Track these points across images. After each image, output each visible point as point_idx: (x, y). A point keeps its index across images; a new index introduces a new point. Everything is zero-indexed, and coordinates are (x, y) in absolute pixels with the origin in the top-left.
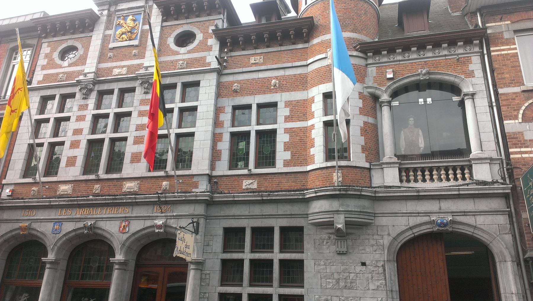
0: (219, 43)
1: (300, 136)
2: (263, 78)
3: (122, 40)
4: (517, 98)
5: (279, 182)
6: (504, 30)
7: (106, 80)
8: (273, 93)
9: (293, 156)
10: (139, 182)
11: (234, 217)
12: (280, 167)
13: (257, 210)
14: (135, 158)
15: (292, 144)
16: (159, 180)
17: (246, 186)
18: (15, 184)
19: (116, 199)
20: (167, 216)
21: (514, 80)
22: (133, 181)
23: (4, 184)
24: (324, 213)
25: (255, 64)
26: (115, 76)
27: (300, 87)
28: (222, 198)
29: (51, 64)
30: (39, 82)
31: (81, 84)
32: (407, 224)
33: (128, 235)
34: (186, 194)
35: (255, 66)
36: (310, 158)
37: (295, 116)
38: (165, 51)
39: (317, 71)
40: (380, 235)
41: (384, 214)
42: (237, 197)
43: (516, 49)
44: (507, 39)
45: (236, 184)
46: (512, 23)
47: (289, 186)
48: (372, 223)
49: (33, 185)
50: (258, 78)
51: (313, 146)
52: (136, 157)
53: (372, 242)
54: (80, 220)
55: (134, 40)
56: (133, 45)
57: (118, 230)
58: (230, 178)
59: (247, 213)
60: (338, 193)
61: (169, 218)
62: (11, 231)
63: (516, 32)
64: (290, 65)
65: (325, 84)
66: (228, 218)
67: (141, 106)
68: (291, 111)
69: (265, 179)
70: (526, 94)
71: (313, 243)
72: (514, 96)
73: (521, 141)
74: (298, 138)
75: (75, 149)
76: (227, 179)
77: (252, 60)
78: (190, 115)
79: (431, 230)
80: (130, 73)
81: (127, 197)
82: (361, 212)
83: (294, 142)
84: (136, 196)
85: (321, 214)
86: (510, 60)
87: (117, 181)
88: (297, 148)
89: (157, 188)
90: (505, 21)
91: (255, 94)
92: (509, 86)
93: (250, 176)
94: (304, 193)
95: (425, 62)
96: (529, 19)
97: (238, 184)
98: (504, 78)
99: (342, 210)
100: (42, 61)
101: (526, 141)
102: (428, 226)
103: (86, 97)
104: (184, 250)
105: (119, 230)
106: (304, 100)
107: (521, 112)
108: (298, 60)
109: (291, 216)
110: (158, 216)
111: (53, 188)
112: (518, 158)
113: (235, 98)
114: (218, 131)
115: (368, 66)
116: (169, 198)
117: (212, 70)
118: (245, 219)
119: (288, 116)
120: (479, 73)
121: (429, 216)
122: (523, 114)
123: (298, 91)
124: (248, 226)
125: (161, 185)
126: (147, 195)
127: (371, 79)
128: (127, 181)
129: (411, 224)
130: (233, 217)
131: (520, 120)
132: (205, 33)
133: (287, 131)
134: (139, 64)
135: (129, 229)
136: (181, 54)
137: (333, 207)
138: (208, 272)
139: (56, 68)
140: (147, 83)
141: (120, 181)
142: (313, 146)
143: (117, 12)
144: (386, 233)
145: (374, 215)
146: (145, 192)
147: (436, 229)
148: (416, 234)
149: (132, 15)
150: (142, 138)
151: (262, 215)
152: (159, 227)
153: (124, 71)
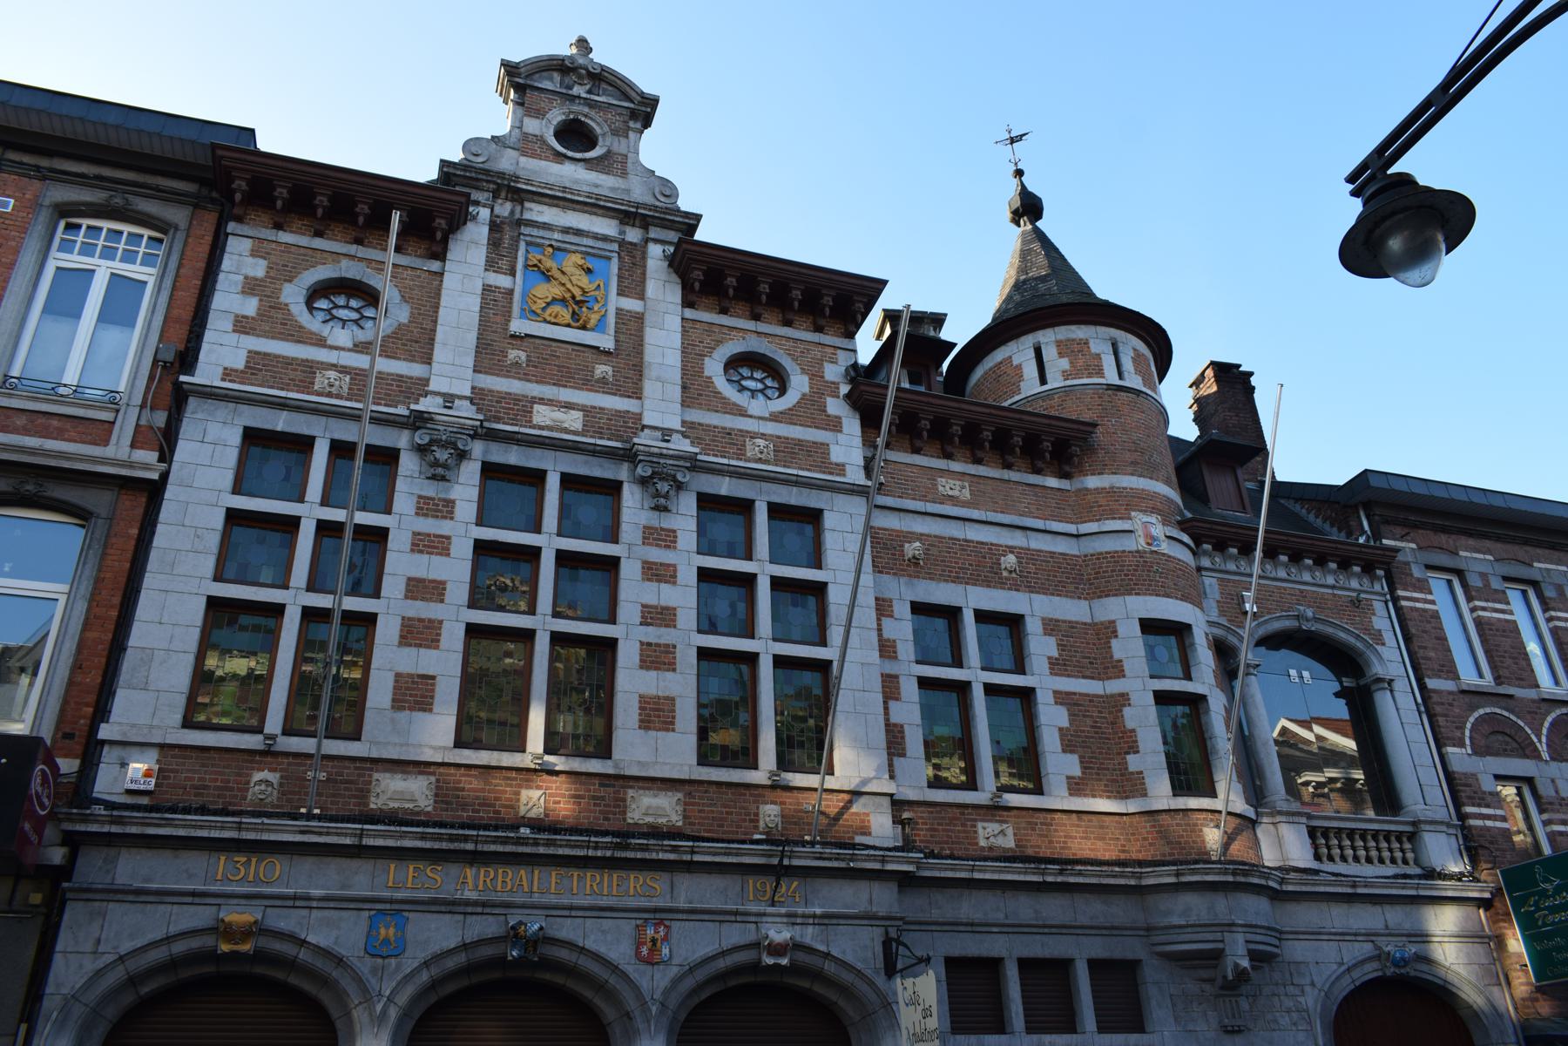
0: (858, 416)
1: (1092, 717)
2: (977, 542)
3: (553, 320)
4: (1455, 703)
5: (1065, 837)
6: (1410, 560)
7: (520, 436)
10: (680, 795)
11: (972, 927)
12: (1058, 798)
13: (1024, 908)
14: (656, 714)
15: (1079, 736)
16: (745, 795)
17: (988, 838)
18: (162, 747)
19: (627, 847)
20: (795, 915)
21: (1443, 666)
22: (660, 789)
23: (103, 742)
24: (1199, 929)
25: (952, 500)
26: (541, 428)
27: (1071, 587)
29: (273, 320)
30: (228, 374)
31: (429, 425)
32: (1339, 960)
33: (674, 971)
34: (856, 852)
35: (953, 505)
36: (1127, 780)
37: (1072, 661)
38: (701, 395)
39: (1111, 557)
40: (1298, 985)
42: (980, 871)
44: (1419, 580)
46: (1420, 548)
47: (1090, 849)
48: (1275, 956)
49: (252, 762)
50: (966, 541)
51: (1134, 749)
53: (1289, 1003)
54: (484, 907)
55: (592, 330)
56: (598, 348)
57: (633, 953)
60: (1230, 878)
62: (169, 939)
63: (1429, 567)
64: (1039, 524)
66: (955, 928)
67: (647, 548)
69: (1029, 823)
70: (1467, 698)
71: (1170, 1005)
73: (1475, 793)
74: (1089, 722)
75: (422, 651)
76: (932, 812)
77: (946, 486)
78: (795, 605)
79: (1380, 974)
80: (594, 432)
81: (665, 843)
82: (1268, 928)
84: (696, 844)
85: (1189, 930)
87: (601, 785)
89: (745, 820)
90: (1409, 541)
91: (967, 583)
92: (1440, 677)
93: (994, 810)
94: (1141, 873)
95: (1302, 591)
96: (1440, 548)
97: (965, 832)
98: (1429, 659)
99: (1240, 922)
100: (228, 300)
101: (1484, 793)
102: (1375, 965)
103: (440, 474)
104: (923, 1027)
105: (638, 953)
106: (1085, 624)
107: (1467, 733)
108: (1051, 516)
109: (1111, 930)
110: (764, 915)
114: (890, 668)
115: (1204, 573)
116: (800, 857)
117: (855, 487)
118: (1000, 935)
119: (1056, 659)
121: (1372, 941)
122: (1471, 738)
123: (1067, 596)
124: (1011, 957)
125: (757, 814)
126: (733, 841)
128: (643, 788)
131: (1470, 751)
132: (816, 376)
133: (1062, 698)
134: (620, 412)
135: (670, 951)
136: (751, 416)
139: (299, 342)
140: (667, 480)
141: (614, 786)
142: (1134, 749)
143: (526, 225)
144: (1308, 981)
145: (1278, 935)
146: (705, 831)
147: (1391, 971)
148: (1357, 984)
149: (581, 252)
151: (1045, 926)
152: (777, 950)
153: (574, 420)
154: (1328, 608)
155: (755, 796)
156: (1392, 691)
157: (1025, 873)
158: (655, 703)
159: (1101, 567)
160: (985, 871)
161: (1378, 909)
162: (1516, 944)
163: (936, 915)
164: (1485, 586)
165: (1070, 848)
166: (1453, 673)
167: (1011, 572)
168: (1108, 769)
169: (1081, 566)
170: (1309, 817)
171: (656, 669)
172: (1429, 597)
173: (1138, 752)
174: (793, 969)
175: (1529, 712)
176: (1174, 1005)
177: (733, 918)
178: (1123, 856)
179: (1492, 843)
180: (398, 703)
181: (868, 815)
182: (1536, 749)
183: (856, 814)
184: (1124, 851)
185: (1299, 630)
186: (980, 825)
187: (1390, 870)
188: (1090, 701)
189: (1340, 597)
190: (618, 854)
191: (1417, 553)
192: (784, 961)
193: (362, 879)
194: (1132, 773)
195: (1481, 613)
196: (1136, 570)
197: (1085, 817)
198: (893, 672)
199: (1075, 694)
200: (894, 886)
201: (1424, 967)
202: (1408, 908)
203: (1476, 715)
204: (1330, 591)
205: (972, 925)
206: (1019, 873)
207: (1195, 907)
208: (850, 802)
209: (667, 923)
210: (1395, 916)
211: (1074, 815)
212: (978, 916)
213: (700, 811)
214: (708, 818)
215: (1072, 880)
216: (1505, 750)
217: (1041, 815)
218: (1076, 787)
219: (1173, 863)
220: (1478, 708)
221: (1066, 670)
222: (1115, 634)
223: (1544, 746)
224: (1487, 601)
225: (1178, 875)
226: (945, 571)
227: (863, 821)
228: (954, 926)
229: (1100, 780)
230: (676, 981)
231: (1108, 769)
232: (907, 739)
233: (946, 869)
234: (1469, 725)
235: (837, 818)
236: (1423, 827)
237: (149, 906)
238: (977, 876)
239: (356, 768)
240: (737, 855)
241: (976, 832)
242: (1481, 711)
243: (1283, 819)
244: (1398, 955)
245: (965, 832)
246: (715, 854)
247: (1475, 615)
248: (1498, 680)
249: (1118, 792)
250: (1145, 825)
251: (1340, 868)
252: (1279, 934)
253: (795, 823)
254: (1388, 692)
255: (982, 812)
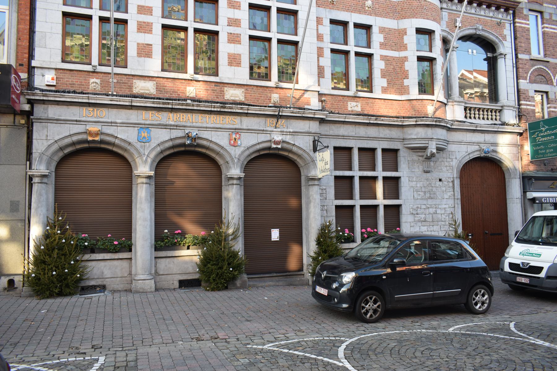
1: (393, 65)
4: (527, 64)
8: (368, 15)
9: (389, 84)
10: (243, 90)
11: (344, 137)
12: (377, 93)
13: (362, 131)
14: (234, 60)
19: (225, 108)
20: (283, 132)
21: (526, 49)
22: (236, 87)
23: (34, 67)
27: (391, 15)
28: (334, 118)
32: (466, 151)
33: (242, 149)
36: (403, 88)
41: (454, 142)
42: (348, 118)
43: (528, 24)
44: (525, 15)
45: (342, 105)
48: (445, 149)
49: (89, 75)
51: (407, 77)
52: (234, 59)
53: (447, 164)
58: (335, 98)
59: (353, 134)
60: (434, 123)
61: (285, 133)
62: (70, 136)
63: (530, 10)
65: (417, 19)
66: (338, 137)
68: (385, 38)
69: (367, 103)
70: (532, 62)
72: (526, 62)
74: (392, 67)
75: (146, 34)
78: (286, 19)
79: (479, 156)
81: (239, 106)
83: (389, 70)
84: (249, 107)
85: (417, 140)
86: (525, 32)
87: (215, 86)
88: (391, 76)
89: (266, 99)
91: (352, 12)
92: (524, 54)
93: (355, 97)
95: (479, 19)
96: (537, 3)
97: (343, 105)
102: (478, 153)
105: (230, 143)
106: (395, 29)
107: (529, 75)
109: (391, 139)
111: (124, 83)
112: (525, 109)
113: (332, 10)
114: (321, 45)
115: (443, 10)
116: (285, 112)
120: (508, 38)
122: (530, 77)
123: (389, 18)
125: (270, 97)
126: (262, 106)
127: (445, 23)
128: (229, 87)
129: (469, 151)
130: (343, 137)
131: (528, 82)
133: (383, 58)
137: (427, 135)
138: (324, 187)
141: (220, 86)
142: (407, 77)
144: (454, 157)
146: (252, 102)
148: (471, 158)
150: (238, 37)
151: (368, 137)
152: (277, 143)
154: (488, 26)
155: (270, 91)
156: (505, 58)
157: (364, 120)
158: (233, 56)
159: (404, 7)
160: (349, 119)
161: (483, 134)
162: (527, 147)
163: (331, 133)
164: (550, 18)
165: (380, 112)
166: (528, 52)
167: (369, 8)
168: (397, 84)
169: (396, 6)
170: (466, 103)
171: (234, 43)
172: (528, 22)
173: (408, 78)
174: (282, 149)
175: (553, 68)
176: (408, 163)
177: (262, 132)
178: (398, 115)
179: (528, 114)
180: (139, 55)
181: (310, 98)
182: (552, 82)
183: (306, 98)
184: (398, 113)
185: (475, 34)
186: (349, 103)
187: (490, 122)
188: (393, 59)
189: (493, 21)
190: (222, 110)
191: (527, 4)
192: (279, 146)
193: (134, 116)
194: (405, 86)
195: (545, 29)
196: (417, 8)
197: (386, 101)
198: (321, 47)
199: (388, 56)
200: (317, 123)
201: (494, 154)
202: (493, 135)
203: (534, 68)
204: (490, 19)
205: (344, 136)
206: (361, 119)
207: (421, 132)
208: (304, 93)
209: (240, 133)
210: (488, 137)
211: (383, 100)
212: (346, 134)
213: (250, 96)
214: (253, 98)
215: (379, 122)
216: (541, 82)
217: (371, 100)
218: (384, 90)
219: (415, 118)
220: (535, 66)
221: (386, 47)
222: (406, 33)
223: (556, 80)
224: (549, 24)
225: (416, 122)
226: (343, 7)
227: (308, 100)
228: (337, 136)
229: (393, 88)
230: (243, 152)
231: (397, 84)
232: (325, 71)
233: (336, 118)
234: (530, 72)
235: (299, 100)
236: (505, 108)
237: (62, 125)
238: (347, 120)
239: (127, 78)
240: (263, 111)
241: (347, 105)
242: (536, 67)
243: (456, 103)
244: (487, 150)
245: (343, 105)
246: (256, 111)
247: (543, 30)
248: (545, 55)
249: (399, 93)
250: (407, 104)
251: (473, 121)
252: (448, 142)
253: (284, 101)
254: (503, 59)
255: (350, 98)
